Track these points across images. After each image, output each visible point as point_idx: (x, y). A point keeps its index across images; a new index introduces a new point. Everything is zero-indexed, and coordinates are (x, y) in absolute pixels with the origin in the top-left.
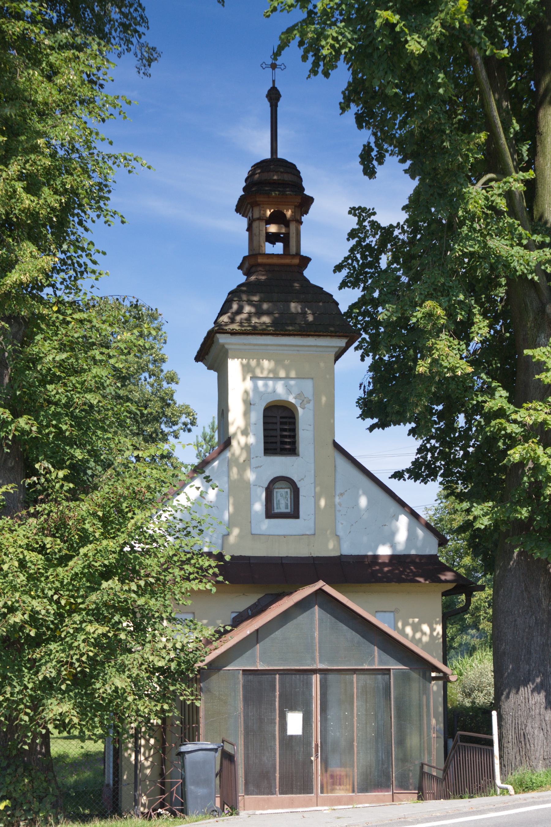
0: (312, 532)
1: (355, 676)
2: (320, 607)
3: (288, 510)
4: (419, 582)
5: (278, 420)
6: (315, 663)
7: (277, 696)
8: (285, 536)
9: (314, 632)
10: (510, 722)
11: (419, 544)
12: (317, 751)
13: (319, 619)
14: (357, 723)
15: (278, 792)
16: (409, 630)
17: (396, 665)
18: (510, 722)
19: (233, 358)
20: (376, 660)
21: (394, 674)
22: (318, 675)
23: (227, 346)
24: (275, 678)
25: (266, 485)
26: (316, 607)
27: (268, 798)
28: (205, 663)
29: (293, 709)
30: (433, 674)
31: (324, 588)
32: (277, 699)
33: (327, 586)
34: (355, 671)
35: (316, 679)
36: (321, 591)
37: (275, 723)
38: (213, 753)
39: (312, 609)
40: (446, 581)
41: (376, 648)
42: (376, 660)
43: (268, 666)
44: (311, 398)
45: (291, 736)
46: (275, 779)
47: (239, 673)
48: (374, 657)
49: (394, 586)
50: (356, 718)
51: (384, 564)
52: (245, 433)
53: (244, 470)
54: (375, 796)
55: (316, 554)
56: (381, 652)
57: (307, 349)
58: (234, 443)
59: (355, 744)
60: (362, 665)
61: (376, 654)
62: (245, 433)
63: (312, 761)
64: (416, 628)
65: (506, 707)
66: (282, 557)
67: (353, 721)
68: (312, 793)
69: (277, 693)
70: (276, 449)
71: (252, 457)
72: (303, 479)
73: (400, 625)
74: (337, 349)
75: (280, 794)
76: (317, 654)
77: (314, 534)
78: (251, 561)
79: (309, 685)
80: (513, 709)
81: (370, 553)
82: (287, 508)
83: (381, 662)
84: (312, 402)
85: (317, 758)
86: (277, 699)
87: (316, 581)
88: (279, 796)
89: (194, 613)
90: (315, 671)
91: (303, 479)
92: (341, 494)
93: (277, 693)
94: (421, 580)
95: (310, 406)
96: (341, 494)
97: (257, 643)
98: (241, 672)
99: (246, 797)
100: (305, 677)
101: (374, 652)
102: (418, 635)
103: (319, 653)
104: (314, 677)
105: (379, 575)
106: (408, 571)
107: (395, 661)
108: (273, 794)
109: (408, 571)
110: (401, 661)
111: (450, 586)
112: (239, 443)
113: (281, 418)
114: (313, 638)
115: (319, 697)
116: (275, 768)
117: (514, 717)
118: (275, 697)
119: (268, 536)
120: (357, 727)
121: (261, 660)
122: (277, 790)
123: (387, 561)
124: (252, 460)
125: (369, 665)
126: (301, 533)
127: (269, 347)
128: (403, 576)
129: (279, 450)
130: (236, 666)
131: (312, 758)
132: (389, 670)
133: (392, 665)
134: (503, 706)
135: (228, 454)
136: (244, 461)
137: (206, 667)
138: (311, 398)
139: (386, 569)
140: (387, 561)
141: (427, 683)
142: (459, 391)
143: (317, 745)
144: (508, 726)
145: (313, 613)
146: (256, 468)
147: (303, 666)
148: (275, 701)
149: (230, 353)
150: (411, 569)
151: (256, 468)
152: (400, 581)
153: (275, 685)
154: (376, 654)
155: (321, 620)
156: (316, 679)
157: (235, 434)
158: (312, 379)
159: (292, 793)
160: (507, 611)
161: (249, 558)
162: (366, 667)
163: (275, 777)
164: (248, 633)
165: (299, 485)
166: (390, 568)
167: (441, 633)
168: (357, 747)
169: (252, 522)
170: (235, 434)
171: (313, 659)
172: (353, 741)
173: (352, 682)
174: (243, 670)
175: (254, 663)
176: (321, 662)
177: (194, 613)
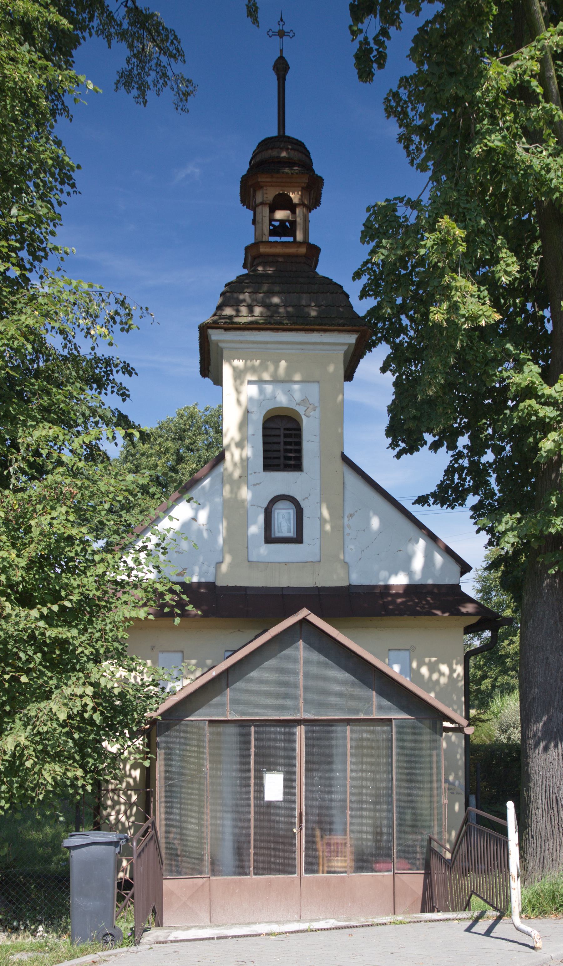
0: (317, 559)
1: (348, 727)
2: (305, 642)
4: (436, 615)
6: (299, 711)
7: (253, 753)
9: (298, 673)
13: (304, 657)
14: (351, 787)
15: (252, 872)
16: (424, 671)
17: (399, 714)
20: (375, 707)
21: (396, 725)
22: (303, 727)
24: (250, 731)
25: (265, 505)
28: (159, 711)
29: (272, 768)
31: (308, 618)
32: (252, 757)
33: (312, 614)
34: (348, 722)
35: (300, 732)
36: (304, 621)
37: (249, 786)
38: (112, 848)
39: (296, 644)
41: (374, 693)
42: (375, 707)
43: (242, 714)
45: (270, 803)
47: (205, 724)
48: (372, 705)
50: (349, 780)
51: (398, 595)
52: (240, 445)
53: (239, 488)
54: (372, 876)
55: (321, 583)
56: (381, 698)
57: (311, 347)
58: (228, 455)
60: (357, 714)
61: (375, 700)
62: (240, 445)
63: (294, 834)
64: (433, 668)
67: (346, 784)
68: (294, 873)
69: (253, 750)
70: (278, 466)
71: (249, 472)
72: (307, 498)
74: (346, 348)
75: (256, 873)
76: (302, 701)
79: (291, 739)
81: (381, 583)
83: (380, 711)
85: (301, 829)
86: (252, 757)
87: (300, 609)
88: (254, 877)
90: (298, 722)
91: (307, 498)
92: (351, 515)
93: (253, 750)
94: (439, 613)
95: (316, 413)
96: (351, 515)
97: (228, 686)
98: (207, 723)
100: (287, 729)
101: (372, 698)
102: (435, 676)
104: (298, 728)
105: (391, 607)
106: (424, 602)
107: (398, 709)
108: (246, 875)
109: (424, 602)
110: (405, 709)
111: (474, 620)
112: (232, 455)
113: (285, 429)
114: (296, 680)
120: (351, 791)
121: (232, 708)
122: (252, 869)
123: (401, 592)
124: (249, 476)
125: (366, 713)
127: (269, 346)
128: (418, 608)
129: (282, 466)
130: (200, 716)
131: (295, 830)
132: (390, 720)
133: (394, 715)
135: (220, 469)
136: (240, 477)
137: (160, 718)
138: (317, 404)
139: (399, 600)
140: (401, 592)
141: (438, 736)
142: (478, 365)
143: (301, 815)
146: (254, 485)
147: (283, 715)
148: (250, 759)
150: (427, 601)
151: (254, 485)
152: (414, 613)
153: (250, 740)
154: (375, 700)
156: (300, 732)
157: (229, 446)
158: (318, 382)
159: (270, 873)
162: (362, 717)
163: (249, 853)
165: (303, 505)
166: (404, 600)
167: (462, 674)
170: (229, 446)
171: (297, 707)
172: (346, 809)
173: (345, 736)
174: (211, 721)
175: (224, 712)
176: (306, 710)
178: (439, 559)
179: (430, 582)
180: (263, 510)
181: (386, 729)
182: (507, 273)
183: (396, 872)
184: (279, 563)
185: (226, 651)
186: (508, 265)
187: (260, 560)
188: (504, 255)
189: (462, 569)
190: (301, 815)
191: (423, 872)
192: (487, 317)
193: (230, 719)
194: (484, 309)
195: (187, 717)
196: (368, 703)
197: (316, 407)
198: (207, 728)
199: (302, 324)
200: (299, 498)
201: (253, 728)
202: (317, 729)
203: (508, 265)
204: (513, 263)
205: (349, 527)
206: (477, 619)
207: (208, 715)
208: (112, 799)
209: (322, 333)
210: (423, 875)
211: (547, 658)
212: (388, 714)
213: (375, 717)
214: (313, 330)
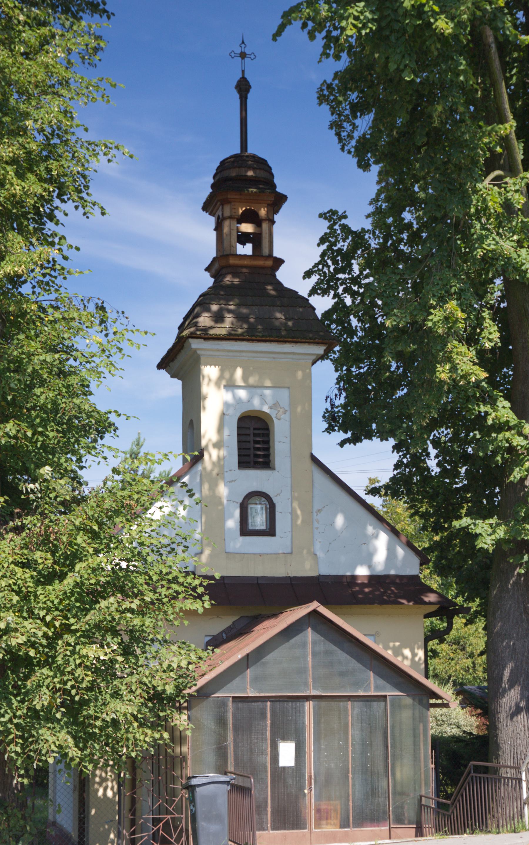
0: (289, 551)
1: (350, 703)
2: (312, 629)
3: (264, 527)
4: (402, 604)
5: (252, 431)
7: (269, 725)
8: (261, 555)
9: (307, 656)
10: (508, 751)
11: (399, 564)
12: (310, 783)
13: (313, 643)
14: (352, 753)
15: (270, 828)
17: (392, 691)
18: (508, 751)
19: (206, 365)
20: (372, 686)
21: (390, 701)
22: (311, 702)
23: (199, 352)
24: (266, 706)
25: (240, 500)
26: (310, 630)
29: (285, 739)
30: (432, 701)
31: (318, 609)
32: (269, 729)
33: (322, 606)
34: (349, 698)
35: (309, 707)
36: (315, 612)
37: (267, 754)
40: (430, 603)
41: (372, 673)
42: (372, 686)
43: (259, 692)
44: (287, 408)
45: (284, 768)
46: (267, 814)
47: (229, 700)
48: (370, 683)
49: (376, 608)
51: (363, 585)
52: (218, 445)
53: (216, 485)
54: (372, 831)
55: (293, 573)
56: (377, 677)
57: (283, 356)
59: (350, 775)
60: (357, 691)
61: (372, 679)
62: (218, 445)
63: (305, 794)
65: (504, 736)
66: (257, 577)
68: (305, 828)
70: (249, 463)
71: (226, 470)
72: (279, 494)
75: (273, 829)
77: (292, 553)
79: (301, 713)
83: (377, 688)
84: (288, 413)
85: (311, 790)
87: (311, 601)
88: (271, 832)
90: (307, 698)
91: (279, 494)
92: (319, 511)
93: (269, 722)
94: (404, 601)
95: (287, 417)
96: (319, 511)
97: (248, 668)
98: (231, 699)
101: (369, 677)
103: (313, 678)
104: (307, 704)
105: (360, 596)
106: (389, 592)
107: (392, 687)
108: (264, 830)
109: (389, 592)
110: (397, 686)
113: (255, 429)
114: (306, 662)
115: (312, 725)
116: (266, 802)
117: (512, 746)
118: (266, 725)
119: (243, 556)
121: (252, 686)
122: (269, 825)
123: (366, 581)
124: (226, 474)
125: (365, 691)
127: (244, 354)
128: (385, 598)
129: (252, 463)
130: (225, 693)
131: (306, 791)
132: (385, 697)
133: (389, 692)
134: (500, 735)
135: (199, 467)
136: (218, 474)
140: (366, 581)
141: (424, 710)
143: (310, 777)
144: (505, 755)
145: (306, 636)
146: (231, 482)
147: (295, 692)
149: (202, 359)
150: (392, 591)
151: (231, 482)
152: (383, 602)
153: (266, 714)
154: (372, 679)
155: (314, 644)
158: (289, 388)
159: (285, 829)
160: (505, 634)
162: (362, 694)
163: (267, 811)
164: (240, 657)
165: (275, 500)
166: (370, 589)
167: (423, 658)
168: (353, 779)
170: (207, 446)
171: (306, 685)
172: (348, 773)
173: (346, 710)
175: (245, 690)
176: (314, 688)
178: (400, 552)
179: (393, 572)
180: (239, 505)
181: (383, 704)
183: (392, 826)
184: (254, 554)
185: (206, 636)
187: (236, 552)
188: (487, 325)
189: (421, 561)
190: (310, 777)
191: (415, 826)
192: (476, 375)
193: (250, 695)
194: (474, 369)
195: (214, 694)
196: (367, 682)
197: (286, 411)
198: (230, 704)
199: (277, 337)
200: (272, 496)
201: (269, 704)
202: (323, 704)
203: (490, 333)
204: (495, 331)
205: (318, 522)
207: (231, 692)
208: (101, 777)
209: (293, 344)
210: (414, 830)
212: (384, 691)
213: (373, 694)
214: (286, 342)
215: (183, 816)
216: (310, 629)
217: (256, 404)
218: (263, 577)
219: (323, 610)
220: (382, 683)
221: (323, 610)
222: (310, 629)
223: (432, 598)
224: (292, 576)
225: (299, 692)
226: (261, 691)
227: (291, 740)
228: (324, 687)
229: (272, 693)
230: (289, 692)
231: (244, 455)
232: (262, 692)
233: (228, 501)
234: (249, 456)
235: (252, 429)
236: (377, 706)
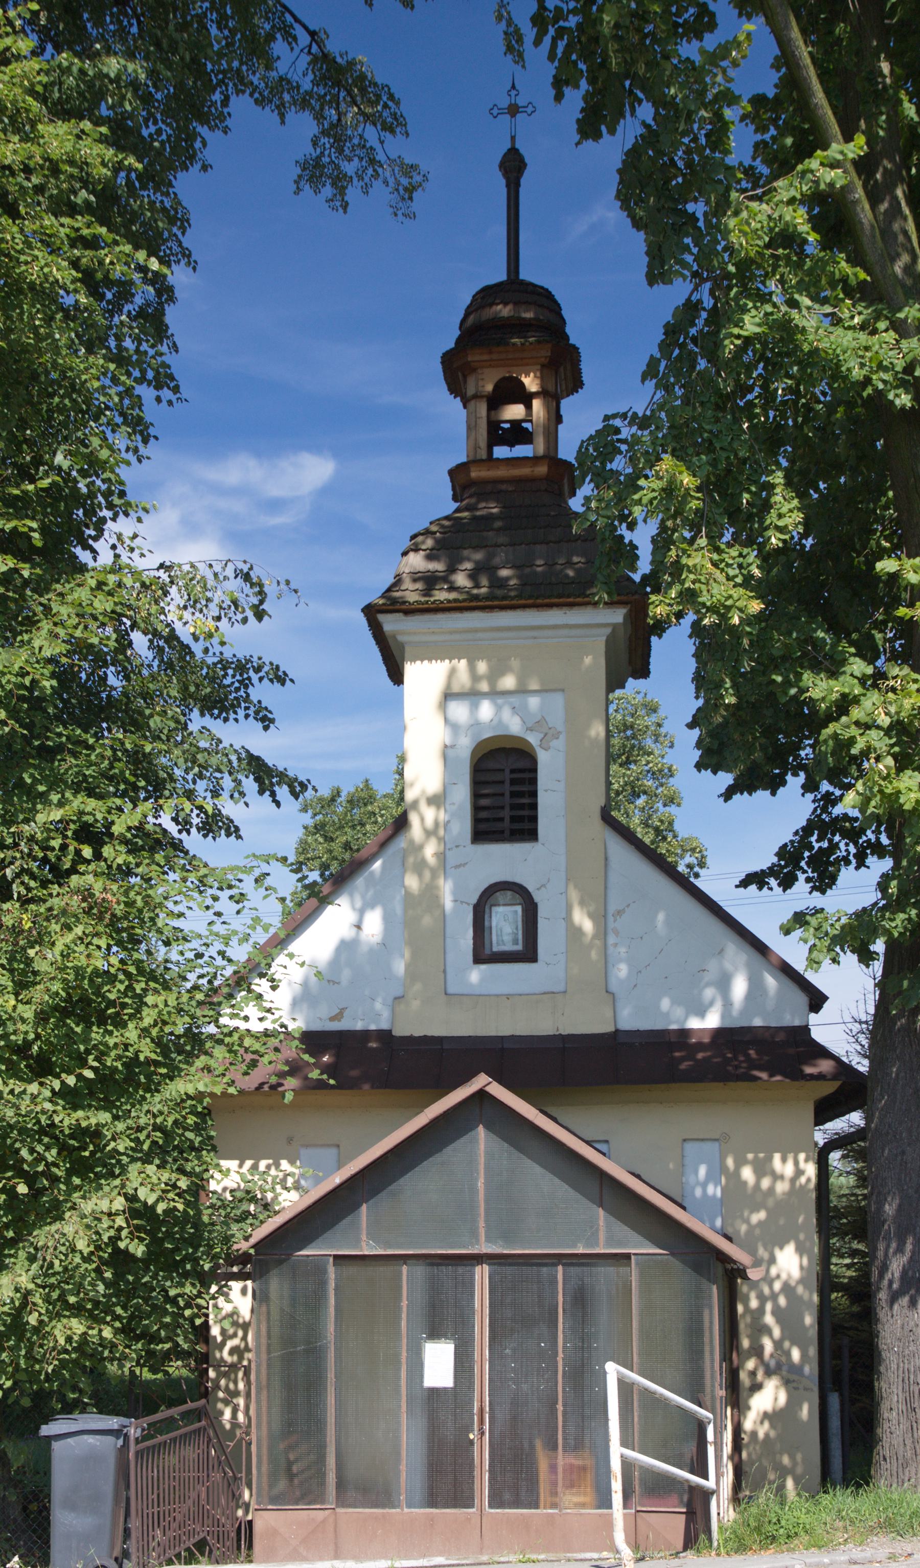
0: (561, 988)
2: (488, 1127)
3: (519, 947)
4: (760, 1078)
5: (507, 776)
6: (478, 1242)
7: (405, 1309)
8: (508, 997)
9: (477, 1179)
11: (770, 1004)
12: (482, 1422)
16: (747, 1174)
17: (642, 1246)
18: (894, 1366)
19: (414, 660)
20: (602, 1235)
22: (486, 1268)
23: (400, 638)
24: (400, 1273)
25: (474, 900)
26: (481, 1129)
27: (383, 1515)
28: (253, 1241)
29: (435, 1334)
31: (488, 1089)
32: (404, 1316)
33: (495, 1084)
34: (559, 1258)
36: (482, 1094)
37: (399, 1362)
39: (473, 1133)
40: (820, 1077)
41: (601, 1212)
42: (602, 1235)
44: (560, 727)
48: (597, 1230)
49: (717, 1089)
50: (561, 1355)
51: (700, 1046)
55: (567, 1028)
56: (612, 1219)
57: (550, 633)
58: (414, 818)
59: (560, 1407)
60: (575, 1246)
61: (601, 1223)
63: (471, 1442)
64: (763, 1168)
66: (502, 1038)
67: (556, 1362)
68: (473, 1507)
69: (404, 1303)
70: (502, 832)
72: (543, 886)
73: (730, 1162)
74: (608, 631)
76: (482, 1224)
77: (565, 992)
78: (446, 1046)
80: (900, 1340)
81: (674, 1027)
82: (515, 942)
83: (609, 1242)
84: (562, 737)
86: (404, 1316)
88: (406, 1510)
89: (338, 1146)
90: (479, 1259)
91: (543, 886)
92: (620, 913)
94: (764, 1075)
95: (559, 743)
96: (620, 913)
98: (331, 1259)
99: (340, 1510)
100: (460, 1270)
102: (766, 1183)
103: (486, 1221)
104: (478, 1269)
106: (742, 1058)
107: (641, 1238)
108: (394, 1507)
109: (742, 1058)
111: (829, 1088)
112: (422, 820)
113: (513, 771)
114: (474, 1190)
115: (487, 1311)
116: (398, 1454)
118: (399, 1308)
119: (475, 998)
120: (564, 1372)
121: (370, 1236)
123: (706, 1040)
125: (586, 1246)
126: (543, 990)
127: (480, 635)
128: (730, 1068)
129: (507, 833)
131: (471, 1436)
132: (627, 1256)
133: (635, 1247)
135: (401, 843)
137: (252, 1251)
138: (560, 727)
139: (700, 1056)
140: (706, 1040)
143: (482, 1410)
144: (890, 1374)
145: (475, 1141)
148: (400, 1318)
149: (408, 651)
150: (747, 1056)
153: (400, 1287)
154: (601, 1223)
155: (489, 1155)
156: (482, 1274)
157: (415, 804)
158: (563, 690)
161: (440, 1040)
162: (581, 1251)
164: (338, 1181)
165: (537, 897)
166: (709, 1054)
167: (814, 1180)
168: (565, 1413)
169: (449, 970)
170: (415, 804)
171: (474, 1234)
172: (557, 1403)
173: (554, 1281)
174: (336, 1257)
175: (357, 1243)
176: (489, 1239)
177: (338, 1146)
178: (771, 982)
179: (758, 1022)
180: (471, 908)
182: (780, 529)
183: (639, 1508)
184: (497, 996)
186: (780, 516)
189: (811, 1000)
190: (482, 1410)
191: (684, 1510)
193: (366, 1253)
195: (300, 1250)
196: (592, 1227)
197: (560, 732)
198: (331, 1270)
199: (530, 597)
200: (531, 889)
202: (509, 1270)
205: (616, 933)
206: (836, 1085)
207: (332, 1247)
209: (565, 609)
210: (684, 1516)
211: (903, 1153)
212: (625, 1247)
213: (602, 1251)
214: (550, 606)
215: (243, 1475)
216: (481, 1126)
217: (514, 726)
218: (512, 1037)
219: (498, 1091)
220: (625, 1230)
221: (498, 1091)
222: (481, 1126)
223: (825, 1066)
224: (566, 1033)
225: (460, 1247)
226: (388, 1245)
227: (447, 1338)
228: (507, 1237)
229: (408, 1248)
230: (441, 1248)
231: (487, 820)
232: (390, 1247)
233: (455, 901)
234: (501, 820)
235: (507, 771)
236: (605, 1273)
